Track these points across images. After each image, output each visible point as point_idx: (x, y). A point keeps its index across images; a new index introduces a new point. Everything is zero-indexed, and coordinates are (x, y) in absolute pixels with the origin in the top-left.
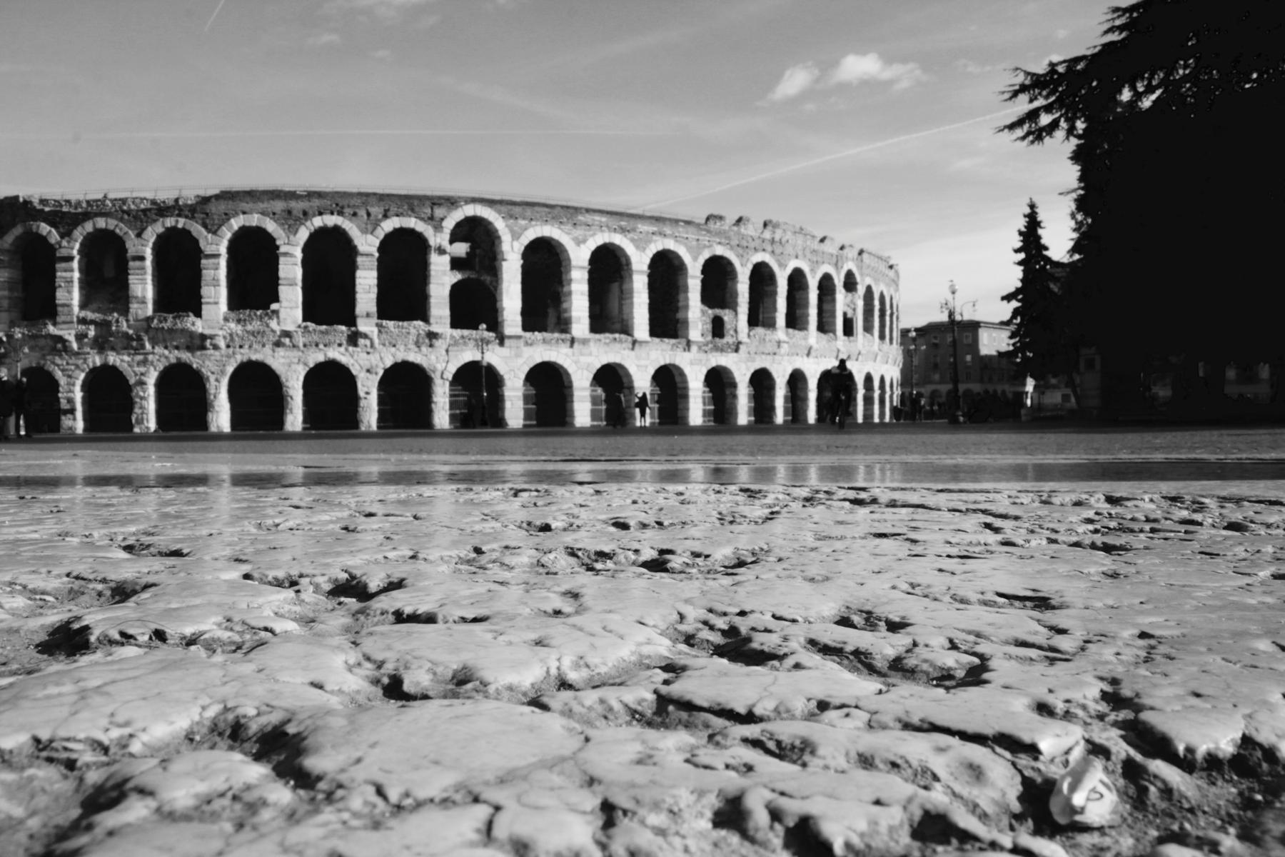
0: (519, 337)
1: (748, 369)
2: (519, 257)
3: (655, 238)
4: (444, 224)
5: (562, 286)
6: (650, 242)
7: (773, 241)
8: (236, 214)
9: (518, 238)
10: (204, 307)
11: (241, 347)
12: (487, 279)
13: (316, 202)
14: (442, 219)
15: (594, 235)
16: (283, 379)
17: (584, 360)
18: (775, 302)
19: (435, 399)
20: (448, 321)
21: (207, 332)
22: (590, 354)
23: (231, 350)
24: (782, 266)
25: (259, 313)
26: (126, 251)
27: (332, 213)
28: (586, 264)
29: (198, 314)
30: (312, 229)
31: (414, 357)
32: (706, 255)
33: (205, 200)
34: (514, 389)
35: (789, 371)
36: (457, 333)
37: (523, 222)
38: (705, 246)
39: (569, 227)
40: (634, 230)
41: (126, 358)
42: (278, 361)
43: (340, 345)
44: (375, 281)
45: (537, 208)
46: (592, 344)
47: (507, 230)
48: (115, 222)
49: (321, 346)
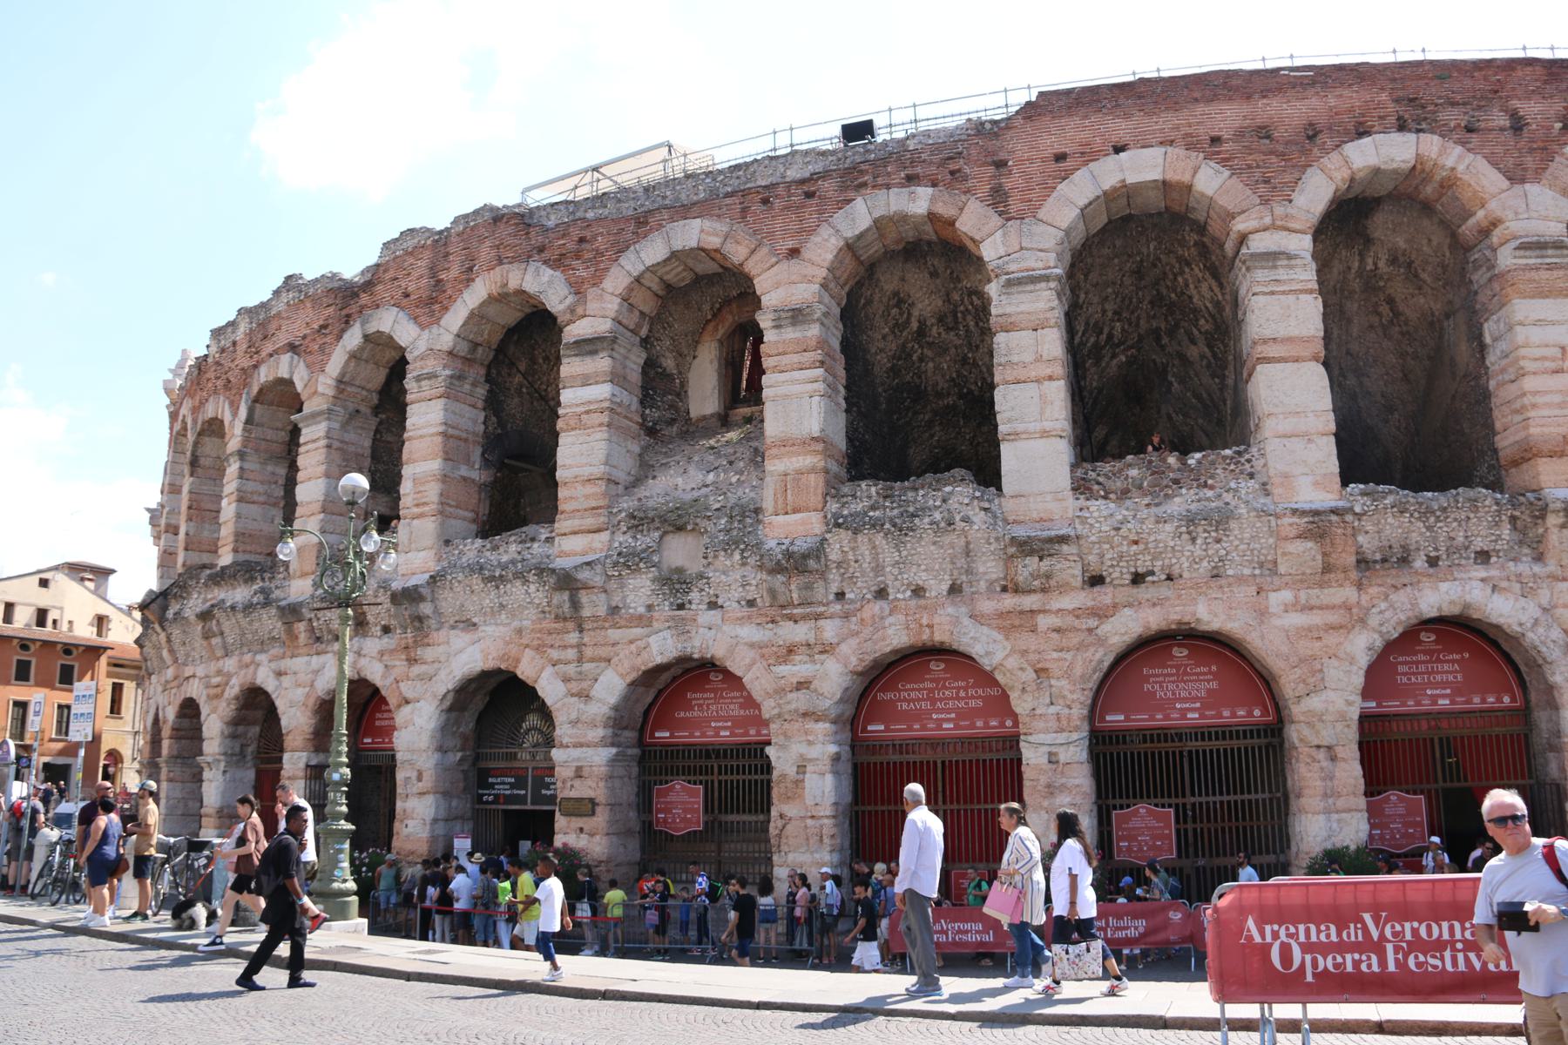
8: (1089, 155)
10: (1006, 450)
11: (1138, 579)
13: (1351, 98)
16: (1289, 683)
21: (1021, 532)
23: (1104, 595)
25: (1194, 458)
26: (756, 302)
27: (1402, 127)
29: (988, 474)
30: (1346, 174)
33: (984, 133)
41: (749, 632)
42: (1274, 626)
43: (1484, 557)
48: (721, 227)
49: (1419, 563)
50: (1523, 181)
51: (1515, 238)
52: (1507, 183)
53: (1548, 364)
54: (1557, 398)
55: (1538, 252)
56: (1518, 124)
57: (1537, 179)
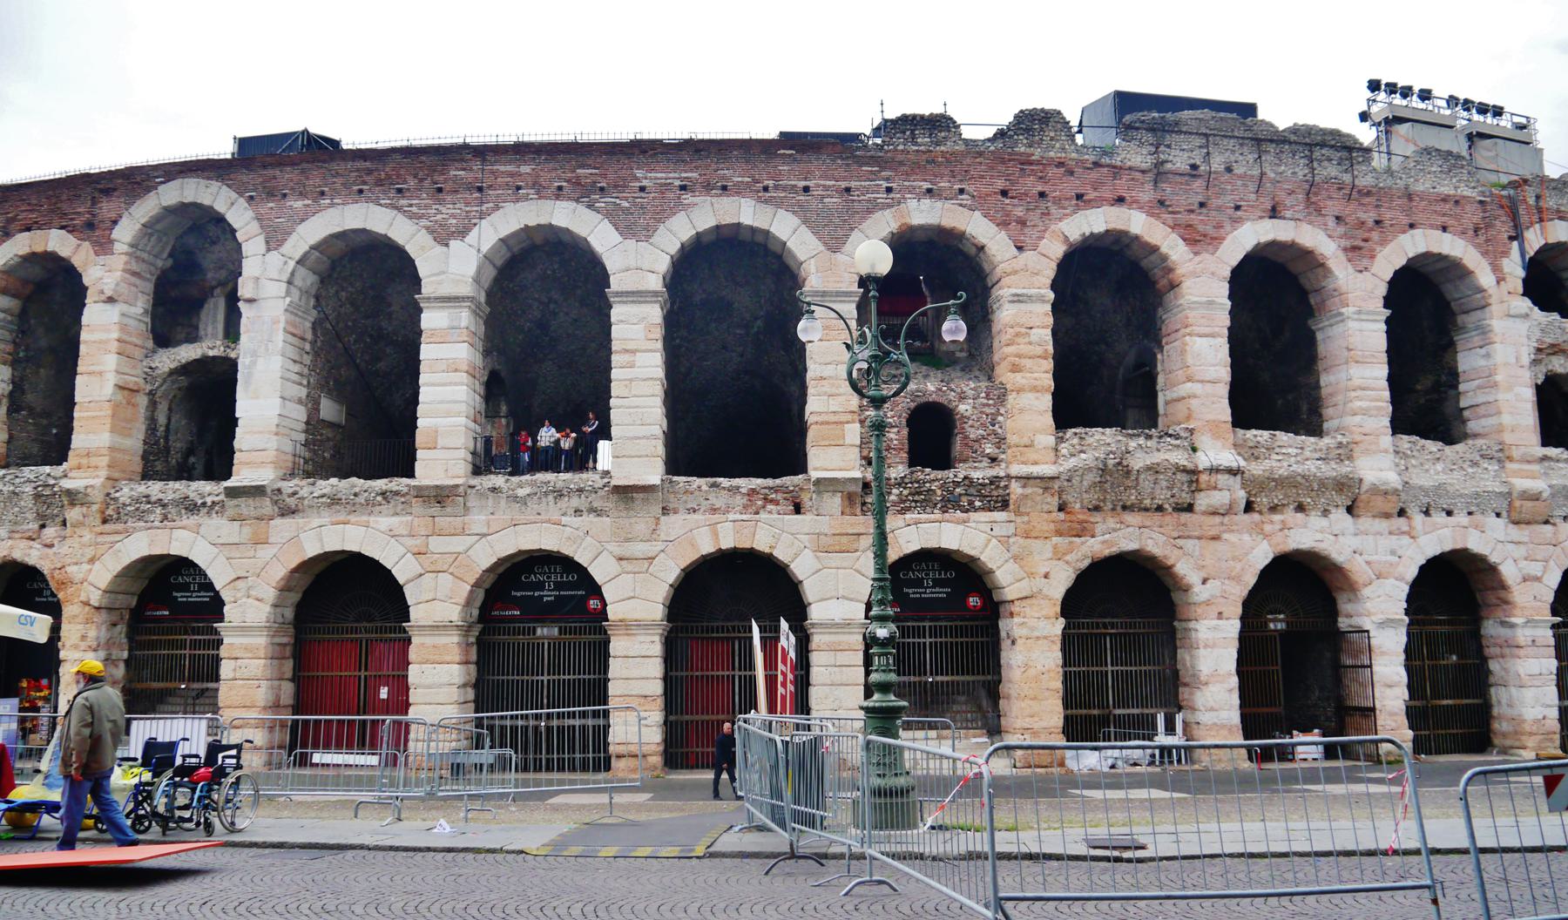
1: (1058, 555)
3: (688, 198)
4: (116, 234)
6: (678, 207)
7: (1159, 173)
9: (281, 243)
14: (115, 222)
15: (497, 208)
19: (62, 655)
22: (463, 532)
34: (244, 630)
35: (1262, 556)
37: (299, 204)
38: (872, 208)
46: (473, 502)
47: (255, 227)
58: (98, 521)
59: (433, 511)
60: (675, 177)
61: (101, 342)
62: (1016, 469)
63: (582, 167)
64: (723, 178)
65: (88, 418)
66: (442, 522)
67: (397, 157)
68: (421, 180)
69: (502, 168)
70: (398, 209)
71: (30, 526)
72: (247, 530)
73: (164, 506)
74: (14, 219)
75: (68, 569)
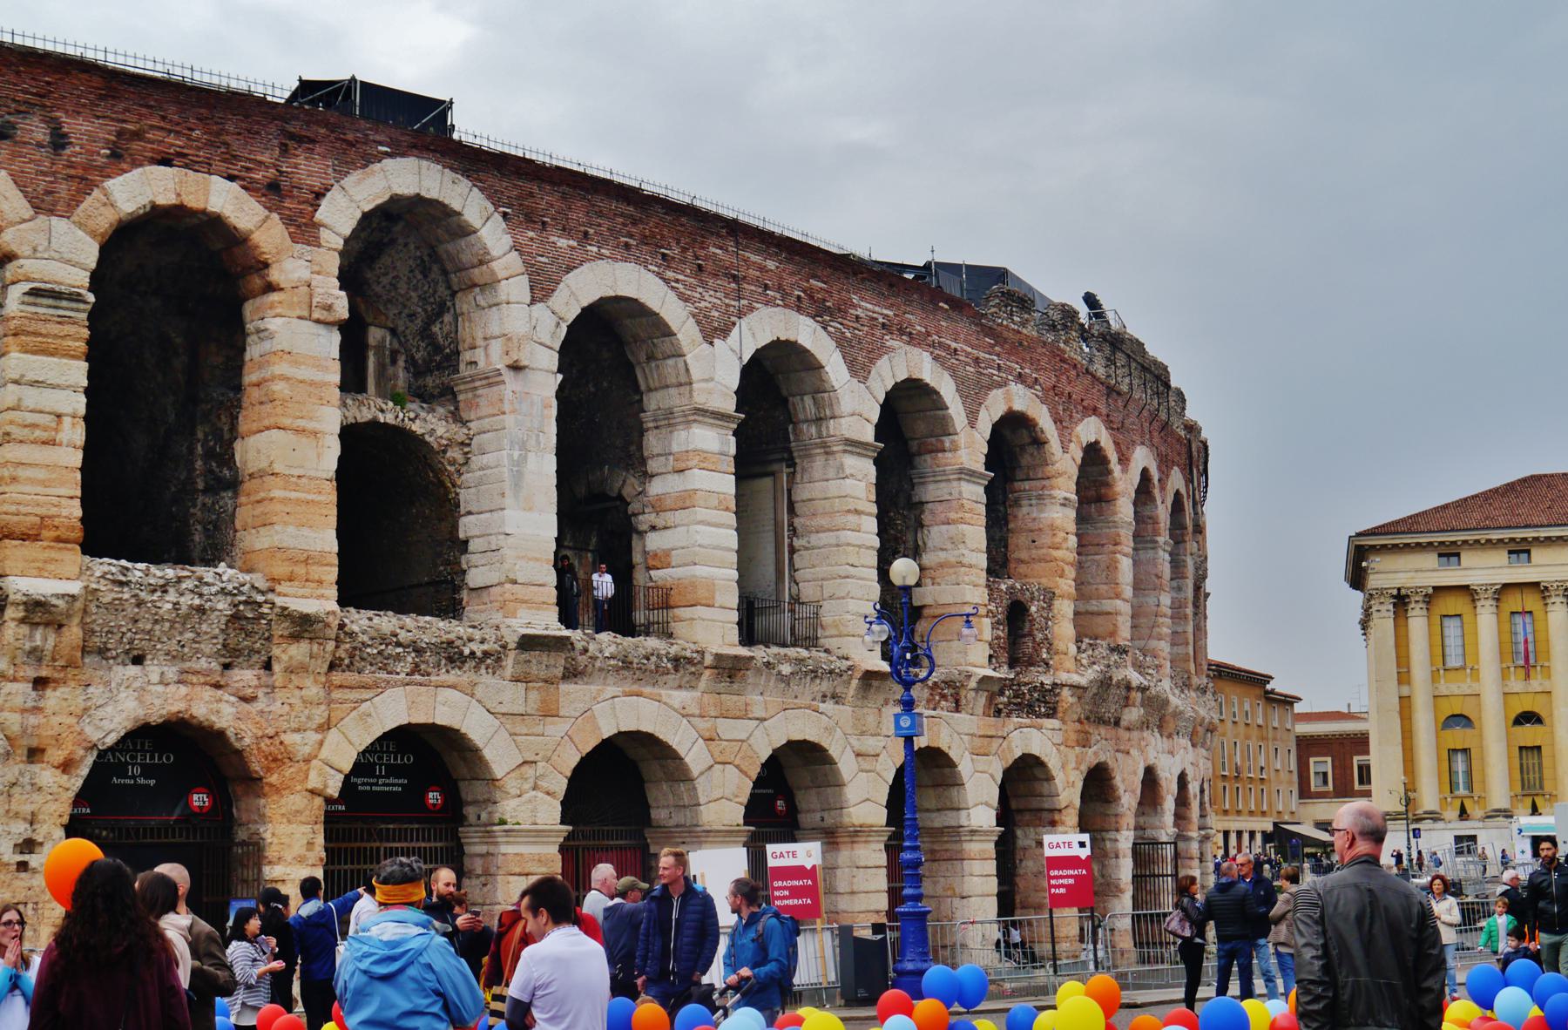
0: (561, 644)
2: (551, 360)
3: (891, 342)
4: (323, 213)
5: (647, 476)
12: (430, 424)
14: (319, 195)
15: (751, 309)
17: (730, 729)
18: (1112, 567)
20: (333, 574)
22: (745, 717)
24: (1124, 460)
28: (729, 405)
31: (216, 709)
32: (994, 407)
36: (360, 621)
37: (563, 243)
39: (685, 277)
40: (840, 311)
44: (80, 403)
45: (602, 203)
50: (51, 212)
51: (28, 280)
52: (28, 212)
53: (38, 433)
54: (41, 474)
55: (50, 302)
56: (59, 141)
57: (67, 215)
58: (326, 666)
59: (722, 686)
60: (883, 312)
61: (312, 384)
62: (1063, 677)
63: (814, 277)
64: (911, 324)
65: (298, 502)
66: (730, 700)
67: (658, 208)
68: (684, 250)
69: (754, 258)
70: (666, 281)
71: (203, 664)
72: (534, 696)
73: (419, 651)
74: (137, 135)
75: (283, 737)
